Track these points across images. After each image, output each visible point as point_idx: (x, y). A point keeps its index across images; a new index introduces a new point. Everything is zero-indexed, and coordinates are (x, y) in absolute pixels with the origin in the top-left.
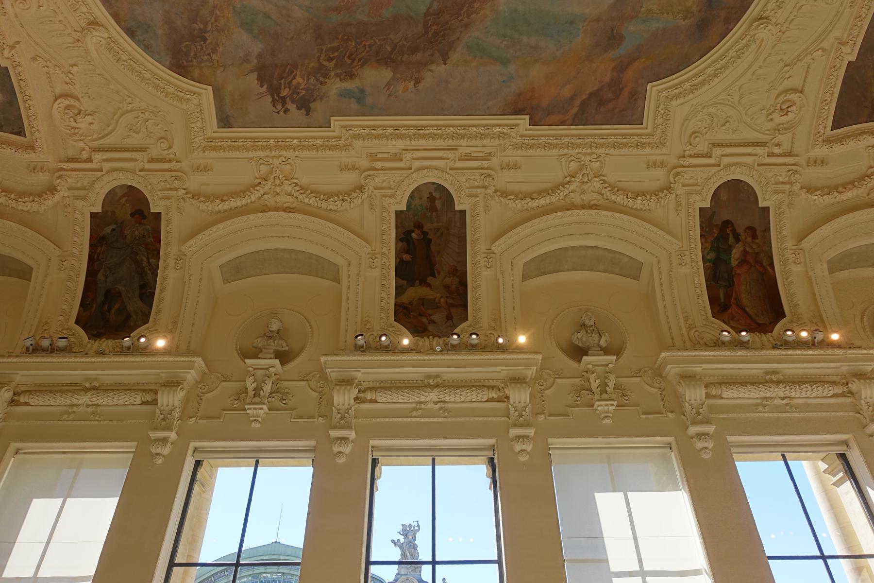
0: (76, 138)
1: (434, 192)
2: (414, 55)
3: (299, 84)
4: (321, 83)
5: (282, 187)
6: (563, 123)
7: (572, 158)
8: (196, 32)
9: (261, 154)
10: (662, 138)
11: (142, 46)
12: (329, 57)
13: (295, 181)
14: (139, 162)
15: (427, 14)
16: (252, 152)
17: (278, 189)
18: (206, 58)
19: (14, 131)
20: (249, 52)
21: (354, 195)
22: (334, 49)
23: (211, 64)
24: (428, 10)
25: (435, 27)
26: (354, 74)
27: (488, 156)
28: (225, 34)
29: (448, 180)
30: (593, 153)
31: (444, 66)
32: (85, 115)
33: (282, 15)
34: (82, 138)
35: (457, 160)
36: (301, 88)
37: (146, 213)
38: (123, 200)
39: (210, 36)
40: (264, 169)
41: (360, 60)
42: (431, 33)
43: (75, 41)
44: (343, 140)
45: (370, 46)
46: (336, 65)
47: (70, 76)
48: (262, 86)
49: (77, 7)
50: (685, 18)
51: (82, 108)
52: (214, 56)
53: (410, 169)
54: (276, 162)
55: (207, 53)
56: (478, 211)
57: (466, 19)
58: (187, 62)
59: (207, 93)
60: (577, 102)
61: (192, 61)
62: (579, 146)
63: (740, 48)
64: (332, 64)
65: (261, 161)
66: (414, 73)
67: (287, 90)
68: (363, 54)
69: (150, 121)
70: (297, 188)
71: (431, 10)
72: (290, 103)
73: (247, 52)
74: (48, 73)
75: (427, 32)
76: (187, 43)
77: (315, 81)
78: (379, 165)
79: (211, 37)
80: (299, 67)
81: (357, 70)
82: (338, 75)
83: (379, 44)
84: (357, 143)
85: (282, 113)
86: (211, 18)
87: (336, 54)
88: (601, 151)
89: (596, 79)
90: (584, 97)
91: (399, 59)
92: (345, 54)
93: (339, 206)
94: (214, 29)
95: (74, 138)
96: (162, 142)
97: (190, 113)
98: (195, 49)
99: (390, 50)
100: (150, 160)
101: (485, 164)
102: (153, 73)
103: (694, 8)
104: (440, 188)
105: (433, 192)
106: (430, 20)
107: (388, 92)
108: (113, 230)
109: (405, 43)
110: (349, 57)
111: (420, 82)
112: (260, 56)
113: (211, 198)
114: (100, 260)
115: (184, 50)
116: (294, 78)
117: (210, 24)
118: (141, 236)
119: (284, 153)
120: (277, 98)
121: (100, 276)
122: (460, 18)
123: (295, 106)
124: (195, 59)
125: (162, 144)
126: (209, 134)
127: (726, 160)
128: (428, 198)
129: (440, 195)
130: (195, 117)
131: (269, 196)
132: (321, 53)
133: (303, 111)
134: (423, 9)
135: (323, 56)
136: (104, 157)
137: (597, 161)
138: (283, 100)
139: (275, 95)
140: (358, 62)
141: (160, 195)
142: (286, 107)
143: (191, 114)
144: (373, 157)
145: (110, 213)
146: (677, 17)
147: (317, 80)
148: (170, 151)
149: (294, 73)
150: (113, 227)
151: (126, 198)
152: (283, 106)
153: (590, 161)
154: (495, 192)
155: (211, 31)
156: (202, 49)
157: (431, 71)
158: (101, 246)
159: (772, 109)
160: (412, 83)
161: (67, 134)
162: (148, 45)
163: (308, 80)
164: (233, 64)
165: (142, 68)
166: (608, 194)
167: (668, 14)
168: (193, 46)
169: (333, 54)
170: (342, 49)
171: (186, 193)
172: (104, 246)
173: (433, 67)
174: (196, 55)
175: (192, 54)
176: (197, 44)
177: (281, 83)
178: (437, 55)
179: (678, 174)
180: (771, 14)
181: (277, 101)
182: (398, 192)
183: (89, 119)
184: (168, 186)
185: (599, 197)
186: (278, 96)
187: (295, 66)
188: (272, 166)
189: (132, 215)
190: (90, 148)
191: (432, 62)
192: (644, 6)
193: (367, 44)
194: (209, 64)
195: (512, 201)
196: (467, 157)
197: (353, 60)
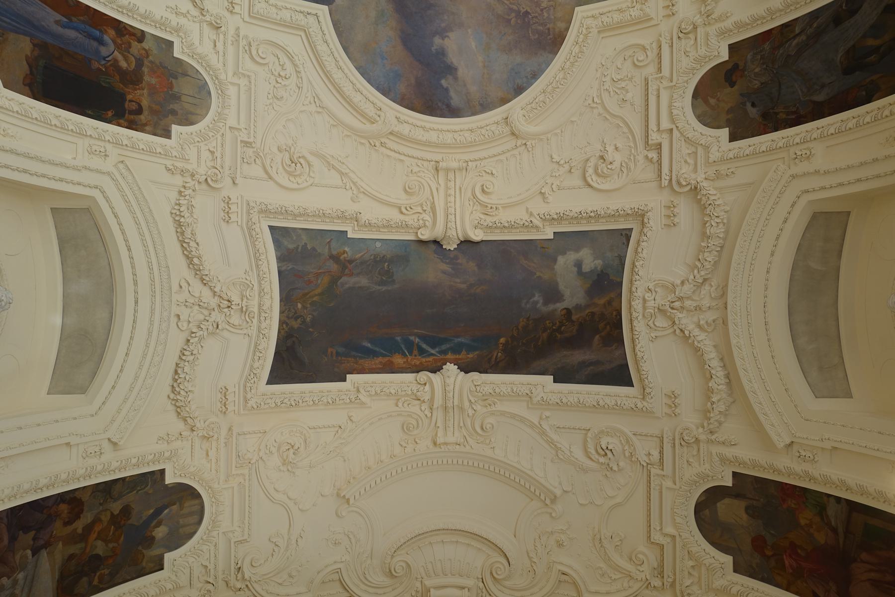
0: (632, 165)
8: (519, 22)
11: (533, 81)
18: (546, 14)
19: (625, 241)
23: (552, 8)
34: (632, 158)
37: (730, 66)
38: (712, 101)
39: (523, 8)
55: (540, 12)
58: (549, 35)
61: (549, 29)
69: (613, 77)
76: (530, 32)
79: (524, 7)
95: (632, 168)
98: (536, 25)
108: (753, 105)
114: (798, 108)
115: (537, 36)
117: (511, 6)
118: (761, 62)
121: (820, 97)
124: (546, 25)
145: (730, 116)
150: (749, 105)
151: (709, 98)
155: (518, 6)
156: (536, 17)
158: (776, 114)
161: (628, 175)
162: (531, 74)
168: (533, 27)
172: (776, 111)
175: (541, 28)
183: (610, 149)
189: (732, 84)
194: (552, 11)
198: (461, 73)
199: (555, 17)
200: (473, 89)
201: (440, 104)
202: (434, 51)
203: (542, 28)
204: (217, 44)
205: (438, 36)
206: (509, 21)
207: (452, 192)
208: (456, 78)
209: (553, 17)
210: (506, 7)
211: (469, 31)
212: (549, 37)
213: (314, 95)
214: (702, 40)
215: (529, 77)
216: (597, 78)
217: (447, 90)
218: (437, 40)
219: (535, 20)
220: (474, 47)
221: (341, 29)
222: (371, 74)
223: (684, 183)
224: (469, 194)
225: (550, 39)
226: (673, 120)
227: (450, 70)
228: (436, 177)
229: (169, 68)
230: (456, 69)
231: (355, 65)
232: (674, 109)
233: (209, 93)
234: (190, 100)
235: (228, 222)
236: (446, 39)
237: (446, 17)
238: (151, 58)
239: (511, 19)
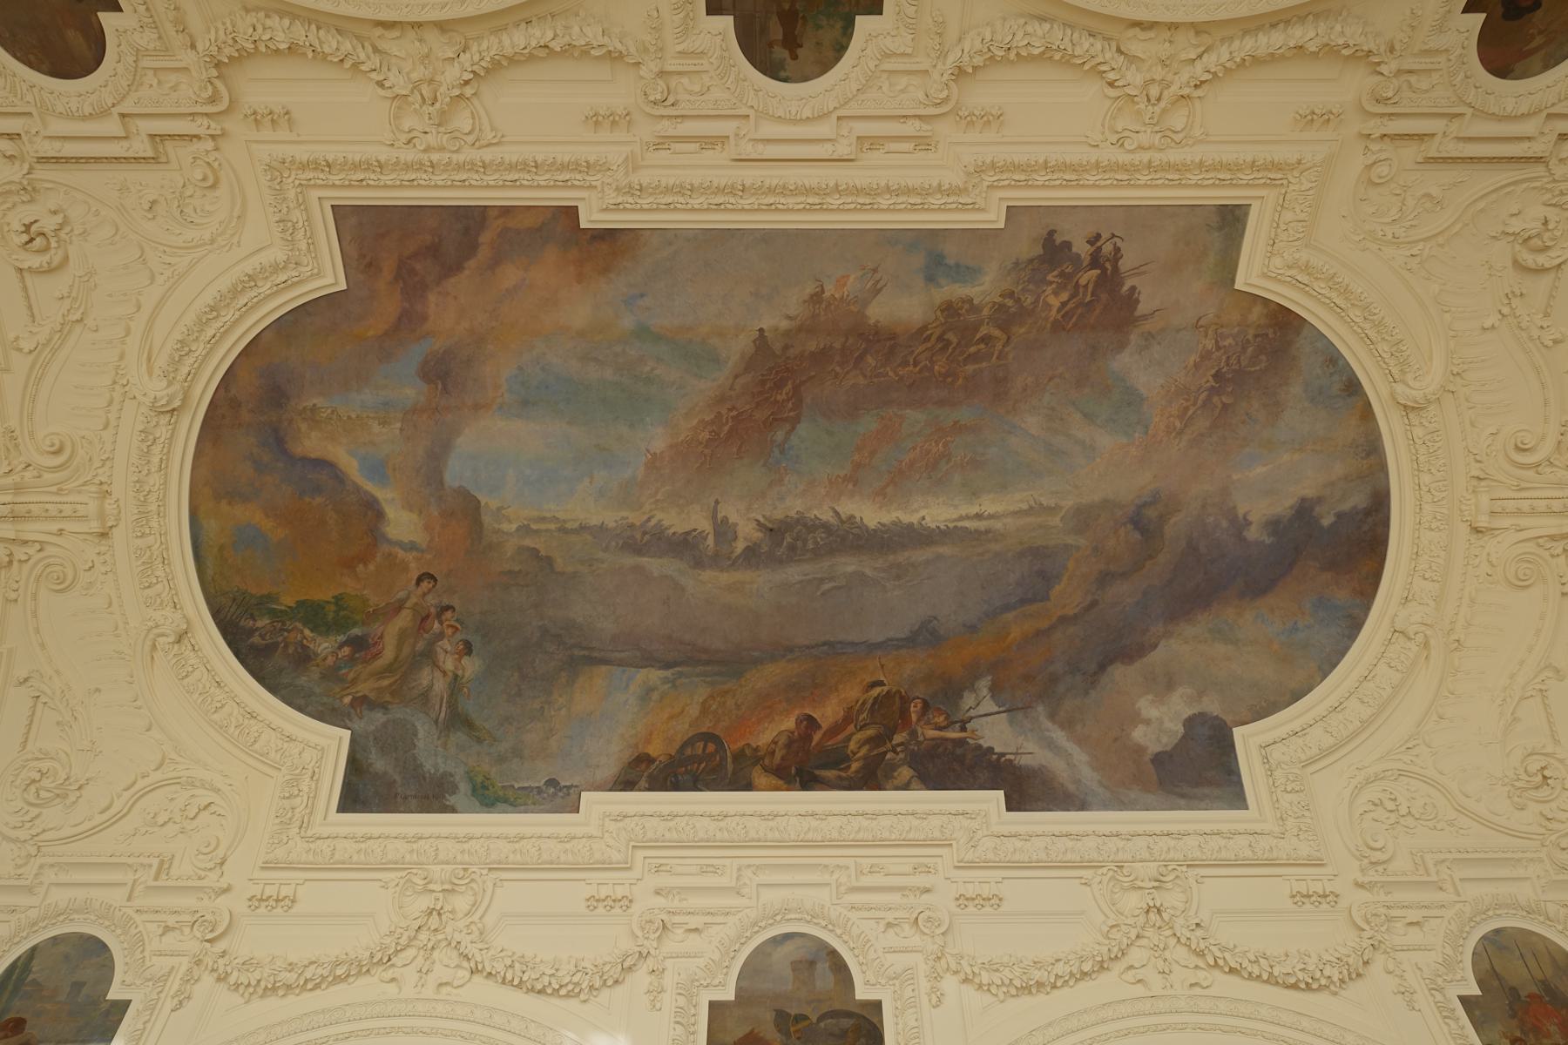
1: (785, 59)
2: (822, 346)
3: (1056, 293)
4: (1011, 295)
5: (1148, 77)
6: (506, 211)
7: (470, 139)
8: (1230, 389)
9: (1174, 156)
10: (279, 180)
11: (1341, 363)
12: (987, 344)
13: (1112, 93)
14: (1454, 135)
15: (796, 420)
16: (1192, 162)
17: (1158, 72)
20: (1140, 353)
21: (978, 61)
22: (975, 358)
23: (1220, 331)
24: (794, 428)
25: (779, 398)
26: (942, 311)
27: (662, 143)
28: (1176, 386)
29: (752, 92)
30: (425, 151)
31: (765, 327)
32: (1519, 233)
33: (1062, 419)
34: (1549, 186)
35: (732, 138)
36: (1054, 286)
38: (1538, 41)
39: (1208, 381)
40: (1178, 120)
41: (928, 339)
42: (789, 386)
43: (1463, 374)
44: (986, 184)
45: (905, 363)
46: (976, 330)
47: (1506, 310)
48: (1133, 288)
49: (1429, 437)
50: (314, 409)
51: (1518, 247)
52: (1209, 344)
53: (839, 118)
54: (1144, 139)
55: (1222, 351)
56: (674, 17)
57: (724, 411)
58: (1267, 335)
59: (1248, 278)
60: (484, 253)
62: (460, 167)
63: (186, 358)
64: (983, 331)
65: (1177, 138)
66: (822, 313)
67: (1083, 282)
68: (920, 349)
70: (1112, 76)
71: (788, 427)
72: (1083, 256)
73: (1143, 353)
74: (1547, 315)
75: (796, 389)
76: (1253, 369)
77: (1023, 299)
78: (910, 128)
79: (1205, 380)
80: (1049, 325)
81: (936, 319)
82: (974, 309)
83: (888, 369)
84: (953, 178)
85: (1105, 236)
86: (1194, 413)
87: (973, 349)
88: (409, 155)
89: (455, 298)
90: (472, 263)
91: (851, 341)
92: (955, 348)
93: (1020, 34)
94: (1194, 394)
96: (1380, 177)
97: (1296, 243)
98: (1242, 358)
99: (869, 357)
100: (1426, 138)
101: (667, 128)
102: (1342, 317)
103: (304, 427)
104: (771, 69)
105: (789, 60)
106: (790, 411)
107: (877, 276)
109: (838, 369)
110: (949, 343)
111: (812, 296)
112: (1122, 346)
113: (1329, 52)
116: (1064, 304)
117: (1200, 402)
119: (1123, 158)
120: (1108, 265)
122: (734, 413)
123: (1074, 250)
125: (1383, 174)
126: (1271, 195)
127: (112, 126)
128: (801, 46)
129: (771, 52)
130: (1291, 232)
131: (1183, 56)
132: (1001, 352)
133: (1058, 239)
134: (803, 429)
135: (999, 346)
136: (1525, 145)
137: (410, 132)
138: (1095, 261)
139: (1109, 272)
140: (931, 334)
141: (1442, 58)
142: (1093, 249)
143: (1298, 239)
144: (923, 143)
146: (329, 411)
147: (1018, 301)
148: (1375, 157)
149: (1062, 313)
152: (1100, 248)
153: (426, 133)
154: (640, 63)
155: (1201, 391)
157: (789, 318)
159: (62, 234)
160: (827, 294)
162: (1328, 366)
163: (1036, 301)
164: (1178, 331)
165: (1359, 327)
166: (363, 56)
167: (349, 417)
168: (1244, 363)
169: (979, 350)
170: (960, 358)
171: (1379, 64)
173: (784, 324)
174: (1244, 349)
176: (1237, 367)
177: (1092, 295)
178: (777, 347)
179: (212, 100)
180: (155, 419)
181: (1108, 260)
182: (872, 65)
183: (1516, 226)
184: (1413, 79)
185: (382, 45)
186: (1104, 270)
187: (1057, 327)
188: (1157, 129)
190: (1547, 164)
191: (787, 333)
192: (398, 432)
193: (911, 368)
194: (1224, 330)
195: (595, 44)
196: (709, 142)
197: (940, 338)
198: (1310, 493)
199: (1239, 325)
200: (1339, 469)
201: (1365, 528)
202: (1271, 539)
203: (1251, 349)
204: (693, 927)
205: (1245, 533)
206: (1225, 406)
207: (1525, 505)
208: (1320, 500)
209: (1236, 330)
210: (1199, 412)
211: (1235, 477)
212: (1270, 336)
213: (1403, 749)
214: (1423, 60)
215: (1332, 371)
216: (1379, 249)
217: (1340, 516)
218: (1253, 534)
219: (1233, 361)
220: (1264, 469)
221: (1264, 704)
222: (1327, 650)
223: (945, 93)
224: (1531, 474)
225: (1275, 333)
226: (822, 116)
227: (1304, 511)
228: (1496, 532)
229: (1507, 1002)
230: (1303, 500)
231: (1319, 680)
232: (801, 114)
233: (1497, 931)
234: (1532, 963)
235: (1000, 900)
236: (1250, 518)
237: (1211, 519)
238: (1518, 1034)
239: (1222, 402)
